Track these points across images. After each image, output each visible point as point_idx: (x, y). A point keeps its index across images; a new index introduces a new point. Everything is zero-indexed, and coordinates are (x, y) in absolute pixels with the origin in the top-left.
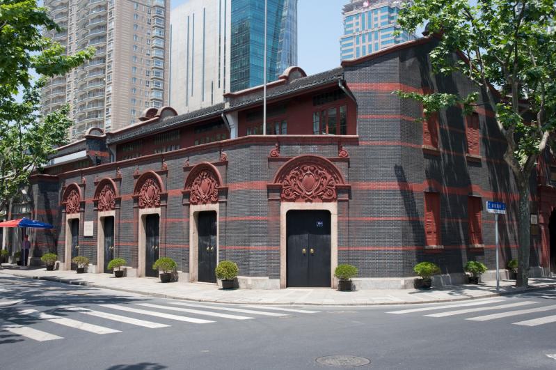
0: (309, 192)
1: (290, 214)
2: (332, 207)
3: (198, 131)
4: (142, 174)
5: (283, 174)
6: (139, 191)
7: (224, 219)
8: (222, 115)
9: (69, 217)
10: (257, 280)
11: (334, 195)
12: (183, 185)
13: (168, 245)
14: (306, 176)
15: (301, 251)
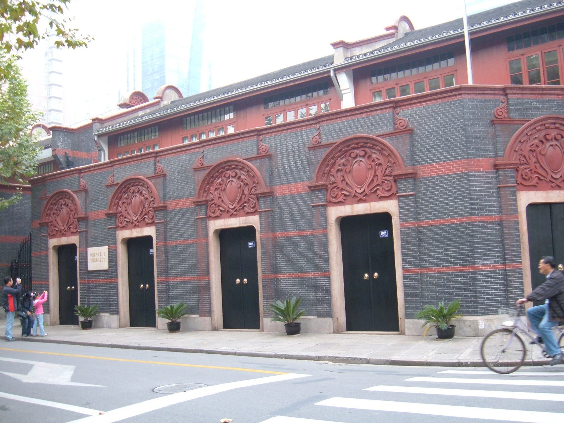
0: (556, 173)
1: (532, 207)
3: (271, 104)
4: (120, 181)
6: (207, 191)
7: (412, 225)
9: (53, 242)
10: (491, 320)
12: (314, 175)
13: (280, 276)
14: (551, 148)
15: (379, 278)
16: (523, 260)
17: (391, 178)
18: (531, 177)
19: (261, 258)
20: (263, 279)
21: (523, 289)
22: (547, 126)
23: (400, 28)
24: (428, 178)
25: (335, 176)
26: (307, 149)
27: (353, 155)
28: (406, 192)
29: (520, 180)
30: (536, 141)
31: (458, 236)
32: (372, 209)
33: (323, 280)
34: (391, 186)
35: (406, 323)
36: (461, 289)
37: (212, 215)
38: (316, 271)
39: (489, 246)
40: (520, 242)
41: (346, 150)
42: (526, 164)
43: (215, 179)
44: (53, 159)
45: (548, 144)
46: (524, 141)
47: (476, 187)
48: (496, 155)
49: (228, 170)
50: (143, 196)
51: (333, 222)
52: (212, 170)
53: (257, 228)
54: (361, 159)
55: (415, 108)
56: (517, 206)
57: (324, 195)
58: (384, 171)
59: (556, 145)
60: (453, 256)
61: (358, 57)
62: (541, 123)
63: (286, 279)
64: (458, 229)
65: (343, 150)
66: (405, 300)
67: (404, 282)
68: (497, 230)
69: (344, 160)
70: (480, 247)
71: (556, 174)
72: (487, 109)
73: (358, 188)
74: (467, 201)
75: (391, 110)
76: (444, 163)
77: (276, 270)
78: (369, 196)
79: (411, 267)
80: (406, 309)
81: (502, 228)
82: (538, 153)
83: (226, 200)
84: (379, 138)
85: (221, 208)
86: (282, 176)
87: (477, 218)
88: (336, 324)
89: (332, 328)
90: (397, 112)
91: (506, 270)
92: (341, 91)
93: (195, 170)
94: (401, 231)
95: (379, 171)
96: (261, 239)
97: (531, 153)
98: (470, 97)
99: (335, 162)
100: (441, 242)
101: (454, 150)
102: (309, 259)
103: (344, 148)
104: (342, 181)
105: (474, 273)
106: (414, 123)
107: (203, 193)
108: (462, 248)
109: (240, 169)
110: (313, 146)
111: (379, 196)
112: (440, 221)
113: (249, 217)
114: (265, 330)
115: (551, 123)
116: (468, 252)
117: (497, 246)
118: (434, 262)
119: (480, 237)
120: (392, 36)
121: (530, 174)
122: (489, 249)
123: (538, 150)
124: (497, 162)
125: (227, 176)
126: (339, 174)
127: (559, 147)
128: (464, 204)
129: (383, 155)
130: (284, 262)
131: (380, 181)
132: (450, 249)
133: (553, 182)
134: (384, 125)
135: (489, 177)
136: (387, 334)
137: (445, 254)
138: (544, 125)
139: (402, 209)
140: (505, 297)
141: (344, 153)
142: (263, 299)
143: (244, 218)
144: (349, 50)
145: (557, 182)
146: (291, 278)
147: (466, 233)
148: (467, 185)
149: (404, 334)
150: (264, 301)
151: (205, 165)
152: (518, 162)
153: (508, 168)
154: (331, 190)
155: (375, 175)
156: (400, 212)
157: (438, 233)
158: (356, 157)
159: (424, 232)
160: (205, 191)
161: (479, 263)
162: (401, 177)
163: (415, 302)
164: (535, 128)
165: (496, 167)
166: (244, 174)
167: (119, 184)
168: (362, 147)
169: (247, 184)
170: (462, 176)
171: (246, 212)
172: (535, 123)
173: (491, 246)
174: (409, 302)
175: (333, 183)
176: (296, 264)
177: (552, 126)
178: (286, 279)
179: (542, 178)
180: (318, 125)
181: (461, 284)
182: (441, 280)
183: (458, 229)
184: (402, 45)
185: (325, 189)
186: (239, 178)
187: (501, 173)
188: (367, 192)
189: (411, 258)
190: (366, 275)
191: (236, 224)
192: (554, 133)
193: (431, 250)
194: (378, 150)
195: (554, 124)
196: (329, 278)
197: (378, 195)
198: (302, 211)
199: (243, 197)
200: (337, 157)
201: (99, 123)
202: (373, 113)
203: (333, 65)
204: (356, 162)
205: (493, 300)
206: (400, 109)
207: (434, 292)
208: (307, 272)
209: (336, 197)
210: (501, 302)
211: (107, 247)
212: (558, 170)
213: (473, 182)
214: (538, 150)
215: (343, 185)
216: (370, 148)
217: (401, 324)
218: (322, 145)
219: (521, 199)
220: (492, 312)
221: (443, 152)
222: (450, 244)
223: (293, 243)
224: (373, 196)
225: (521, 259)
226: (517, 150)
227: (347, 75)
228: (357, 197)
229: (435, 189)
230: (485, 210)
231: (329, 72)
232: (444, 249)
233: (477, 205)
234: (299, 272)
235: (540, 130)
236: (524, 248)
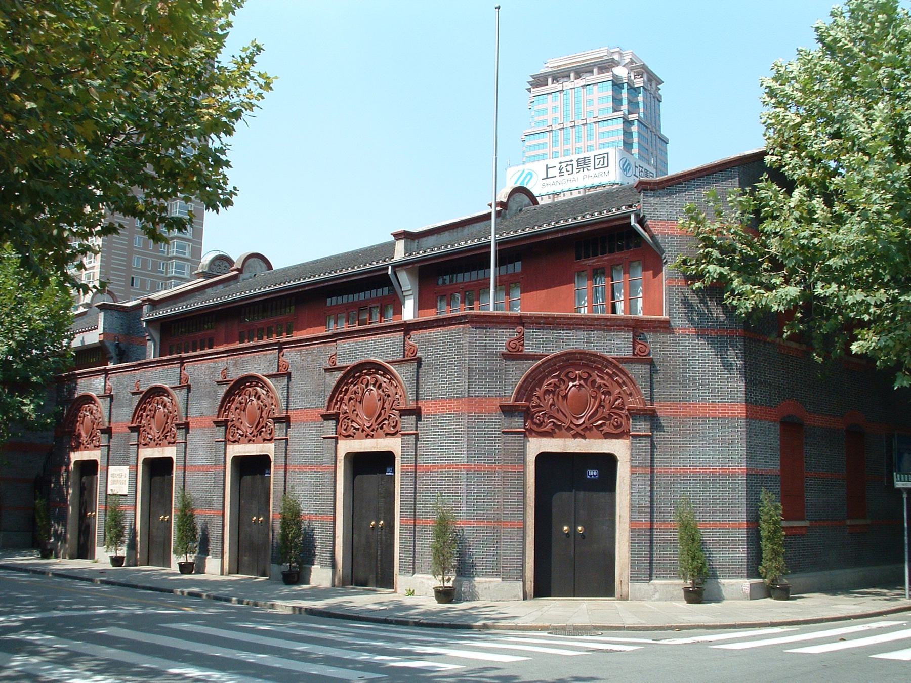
0: (578, 419)
1: (543, 459)
2: (619, 448)
5: (527, 389)
8: (390, 272)
44: (99, 345)
71: (578, 420)
92: (403, 292)
145: (579, 429)
167: (143, 392)
184: (462, 243)
191: (253, 452)
211: (128, 467)
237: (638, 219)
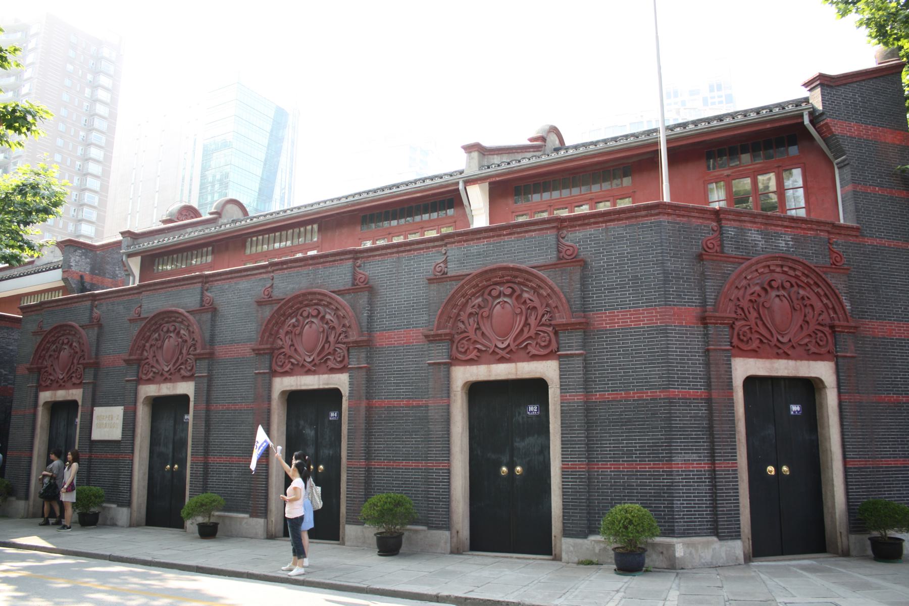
1: (751, 382)
9: (45, 396)
11: (830, 346)
14: (777, 300)
16: (738, 457)
17: (551, 329)
18: (751, 339)
19: (346, 437)
20: (348, 467)
21: (738, 499)
22: (772, 268)
23: (548, 140)
24: (606, 330)
25: (466, 322)
26: (427, 281)
27: (494, 293)
28: (572, 350)
29: (735, 341)
30: (757, 288)
31: (647, 418)
32: (518, 373)
33: (440, 473)
34: (550, 341)
35: (566, 545)
36: (650, 496)
37: (279, 369)
38: (429, 460)
39: (692, 435)
40: (735, 431)
41: (497, 281)
42: (744, 319)
43: (287, 318)
45: (773, 293)
46: (742, 287)
47: (676, 348)
48: (704, 304)
49: (307, 306)
50: (181, 337)
51: (459, 389)
52: (284, 304)
53: (345, 391)
54: (505, 300)
55: (590, 231)
56: (731, 378)
57: (448, 349)
58: (539, 317)
59: (784, 296)
60: (639, 447)
61: (499, 166)
62: (764, 264)
63: (384, 468)
64: (648, 407)
65: (480, 285)
66: (563, 509)
67: (563, 482)
68: (703, 412)
69: (480, 300)
70: (680, 435)
71: (783, 337)
72: (694, 239)
73: (500, 340)
74: (662, 367)
75: (554, 232)
76: (630, 311)
77: (369, 455)
78: (514, 353)
79: (576, 461)
80: (564, 523)
81: (710, 409)
82: (761, 304)
83: (301, 349)
84: (534, 270)
85: (293, 360)
86: (386, 318)
87: (676, 392)
88: (455, 540)
89: (449, 545)
90: (563, 235)
91: (714, 471)
93: (260, 303)
94: (561, 406)
95: (533, 317)
96: (349, 407)
97: (751, 305)
98: (670, 219)
99: (467, 302)
100: (622, 425)
101: (646, 292)
102: (419, 441)
103: (481, 282)
104: (476, 329)
105: (670, 473)
106: (587, 251)
107: (268, 337)
108: (653, 435)
109: (324, 305)
110: (435, 277)
111: (531, 354)
112: (622, 394)
113: (334, 376)
114: (347, 543)
115: (777, 265)
116: (662, 443)
117: (703, 435)
118: (610, 454)
119: (680, 420)
120: (540, 149)
121: (749, 335)
122: (691, 438)
123: (761, 300)
124: (707, 314)
125: (305, 314)
126: (471, 320)
127: (786, 298)
128: (658, 370)
129: (540, 295)
130: (380, 444)
131: (532, 332)
132: (635, 436)
133: (780, 348)
134: (543, 253)
135: (694, 334)
136: (533, 559)
137: (626, 443)
138: (769, 266)
139: (566, 375)
140: (713, 511)
141: (481, 291)
142: (347, 497)
143: (326, 376)
144: (486, 157)
146: (390, 468)
147: (660, 414)
148: (664, 344)
149: (560, 560)
150: (347, 500)
151: (274, 298)
152: (735, 316)
153: (721, 324)
154: (459, 342)
155: (527, 324)
156: (560, 378)
157: (618, 412)
158: (498, 296)
159: (597, 409)
160: (271, 334)
161: (678, 459)
162: (565, 328)
163: (579, 513)
164: (757, 270)
165: (704, 320)
166: (329, 313)
168: (508, 282)
169: (334, 328)
170: (657, 330)
171: (329, 368)
172: (757, 263)
173: (695, 435)
174: (569, 513)
175: (462, 333)
176: (400, 447)
177: (778, 270)
178: (384, 468)
179: (765, 341)
180: (444, 248)
181: (650, 489)
182: (620, 482)
183: (648, 407)
185: (450, 340)
186: (323, 318)
187: (711, 330)
188: (513, 347)
189: (575, 448)
190: (504, 469)
191: (313, 385)
192: (780, 278)
193: (606, 437)
194: (532, 288)
195: (782, 266)
196: (449, 472)
197: (529, 353)
198: (412, 370)
199: (327, 346)
200: (469, 295)
201: (131, 238)
202: (527, 235)
203: (463, 175)
204: (499, 303)
205: (695, 515)
206: (568, 231)
207: (608, 499)
208: (415, 460)
209: (465, 352)
210: (707, 518)
211: (122, 407)
212: (785, 331)
213: (672, 340)
214: (761, 300)
215: (479, 337)
216: (519, 283)
217: (555, 545)
218: (449, 277)
219: (736, 369)
220: (695, 533)
221: (629, 294)
222: (634, 429)
223: (397, 417)
224: (522, 354)
225: (736, 456)
226: (732, 298)
227: (482, 189)
228: (498, 354)
229: (615, 348)
230: (688, 382)
231: (458, 183)
232: (626, 436)
233: (678, 374)
234: (402, 460)
235: (762, 273)
236: (739, 439)
237: (811, 118)
